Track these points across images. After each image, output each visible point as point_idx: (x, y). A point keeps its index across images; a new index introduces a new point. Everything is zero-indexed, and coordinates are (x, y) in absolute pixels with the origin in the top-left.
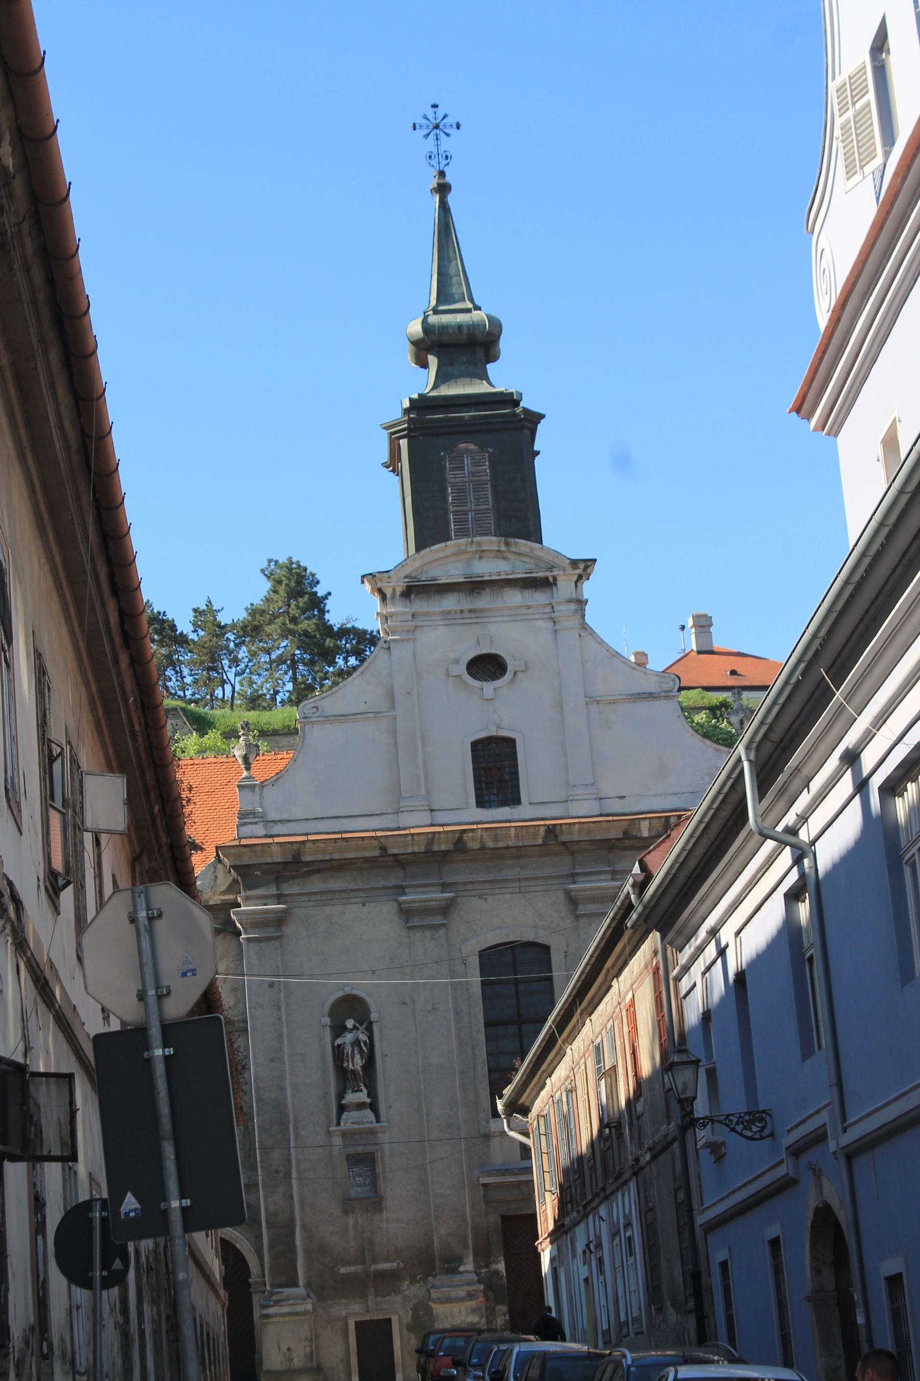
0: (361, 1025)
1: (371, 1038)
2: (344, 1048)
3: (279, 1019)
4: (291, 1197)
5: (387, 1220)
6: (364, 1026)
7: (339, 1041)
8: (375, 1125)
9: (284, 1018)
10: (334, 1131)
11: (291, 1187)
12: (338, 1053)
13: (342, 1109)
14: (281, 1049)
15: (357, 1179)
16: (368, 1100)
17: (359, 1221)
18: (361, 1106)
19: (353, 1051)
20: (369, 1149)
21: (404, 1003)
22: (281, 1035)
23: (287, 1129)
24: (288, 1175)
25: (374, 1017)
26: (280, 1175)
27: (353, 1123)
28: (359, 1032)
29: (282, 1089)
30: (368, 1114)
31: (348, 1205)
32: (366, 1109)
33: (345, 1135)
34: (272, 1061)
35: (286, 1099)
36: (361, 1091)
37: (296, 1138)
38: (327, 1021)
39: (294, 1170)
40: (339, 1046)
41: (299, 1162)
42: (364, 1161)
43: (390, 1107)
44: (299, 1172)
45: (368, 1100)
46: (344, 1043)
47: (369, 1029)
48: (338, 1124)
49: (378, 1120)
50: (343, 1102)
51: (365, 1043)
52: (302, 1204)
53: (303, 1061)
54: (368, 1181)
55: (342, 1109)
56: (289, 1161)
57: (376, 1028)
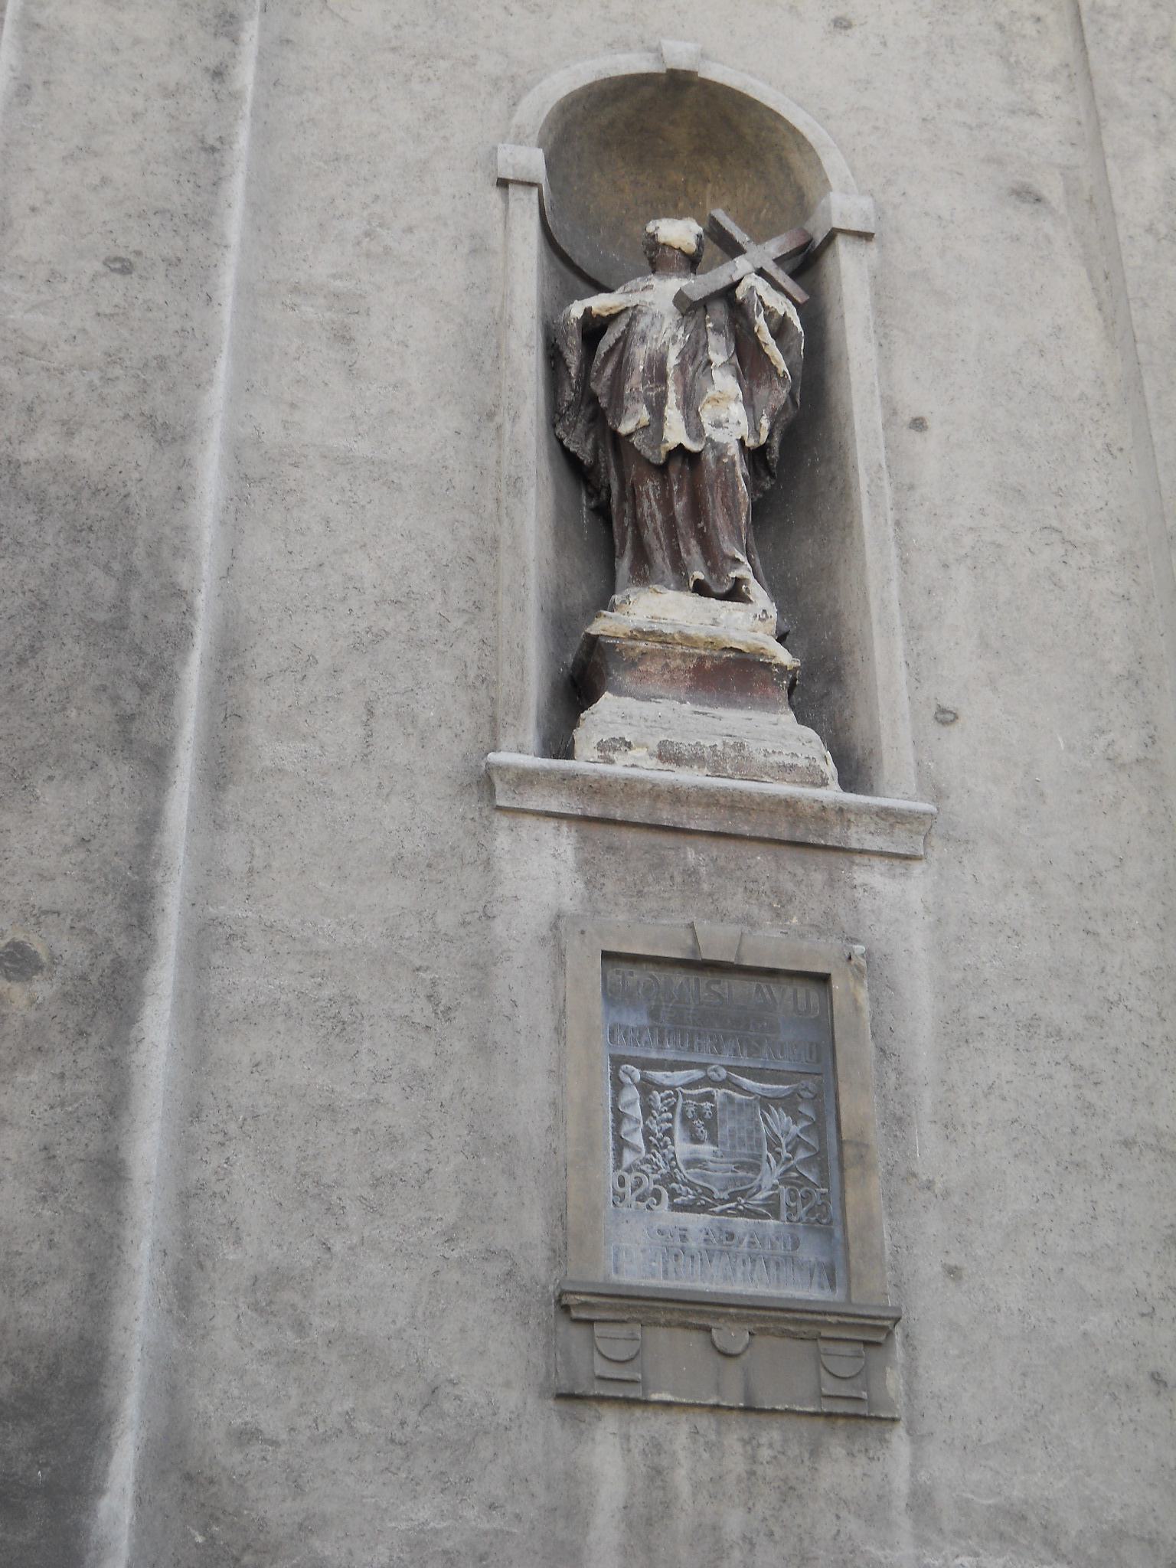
0: (759, 239)
1: (815, 314)
2: (624, 340)
3: (218, 74)
4: (109, 1173)
5: (921, 1502)
6: (774, 248)
7: (601, 303)
8: (832, 793)
9: (246, 76)
10: (525, 778)
11: (115, 1105)
12: (583, 371)
13: (581, 679)
14: (203, 220)
15: (682, 1148)
16: (783, 656)
17: (681, 1478)
18: (727, 674)
19: (694, 355)
20: (770, 943)
21: (1028, 196)
22: (214, 150)
23: (157, 679)
24: (110, 997)
25: (842, 205)
26: (43, 988)
27: (668, 755)
28: (741, 266)
29: (171, 435)
30: (774, 738)
31: (600, 1338)
32: (766, 704)
33: (604, 819)
34: (123, 267)
35: (181, 495)
36: (736, 594)
37: (217, 776)
38: (532, 161)
39: (164, 977)
40: (593, 328)
41: (208, 939)
42: (747, 1028)
43: (946, 717)
44: (199, 1017)
45: (783, 656)
46: (633, 313)
47: (806, 262)
48: (559, 744)
49: (853, 770)
50: (604, 625)
51: (780, 330)
52: (184, 1291)
53: (343, 337)
54: (770, 1176)
55: (581, 679)
56: (138, 903)
57: (850, 272)
